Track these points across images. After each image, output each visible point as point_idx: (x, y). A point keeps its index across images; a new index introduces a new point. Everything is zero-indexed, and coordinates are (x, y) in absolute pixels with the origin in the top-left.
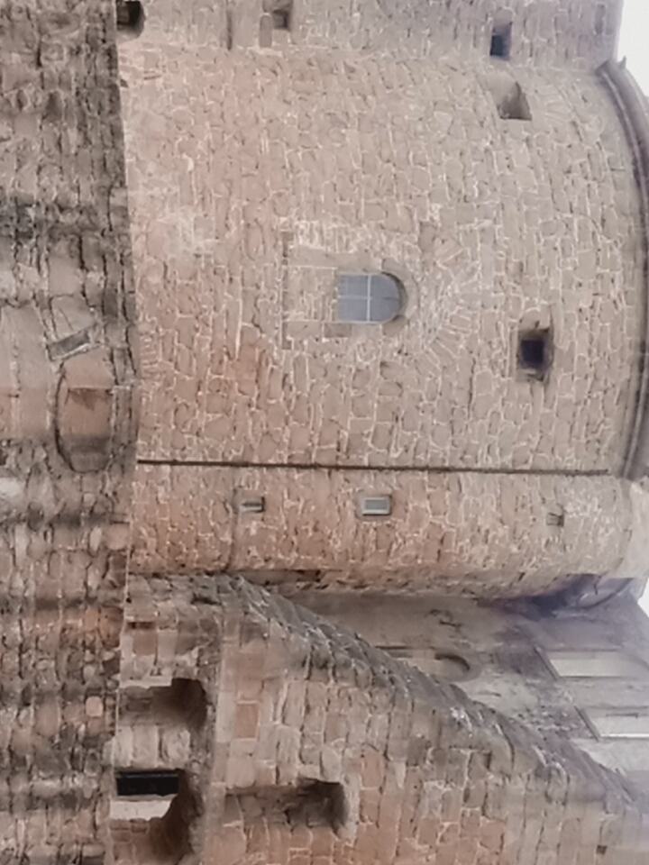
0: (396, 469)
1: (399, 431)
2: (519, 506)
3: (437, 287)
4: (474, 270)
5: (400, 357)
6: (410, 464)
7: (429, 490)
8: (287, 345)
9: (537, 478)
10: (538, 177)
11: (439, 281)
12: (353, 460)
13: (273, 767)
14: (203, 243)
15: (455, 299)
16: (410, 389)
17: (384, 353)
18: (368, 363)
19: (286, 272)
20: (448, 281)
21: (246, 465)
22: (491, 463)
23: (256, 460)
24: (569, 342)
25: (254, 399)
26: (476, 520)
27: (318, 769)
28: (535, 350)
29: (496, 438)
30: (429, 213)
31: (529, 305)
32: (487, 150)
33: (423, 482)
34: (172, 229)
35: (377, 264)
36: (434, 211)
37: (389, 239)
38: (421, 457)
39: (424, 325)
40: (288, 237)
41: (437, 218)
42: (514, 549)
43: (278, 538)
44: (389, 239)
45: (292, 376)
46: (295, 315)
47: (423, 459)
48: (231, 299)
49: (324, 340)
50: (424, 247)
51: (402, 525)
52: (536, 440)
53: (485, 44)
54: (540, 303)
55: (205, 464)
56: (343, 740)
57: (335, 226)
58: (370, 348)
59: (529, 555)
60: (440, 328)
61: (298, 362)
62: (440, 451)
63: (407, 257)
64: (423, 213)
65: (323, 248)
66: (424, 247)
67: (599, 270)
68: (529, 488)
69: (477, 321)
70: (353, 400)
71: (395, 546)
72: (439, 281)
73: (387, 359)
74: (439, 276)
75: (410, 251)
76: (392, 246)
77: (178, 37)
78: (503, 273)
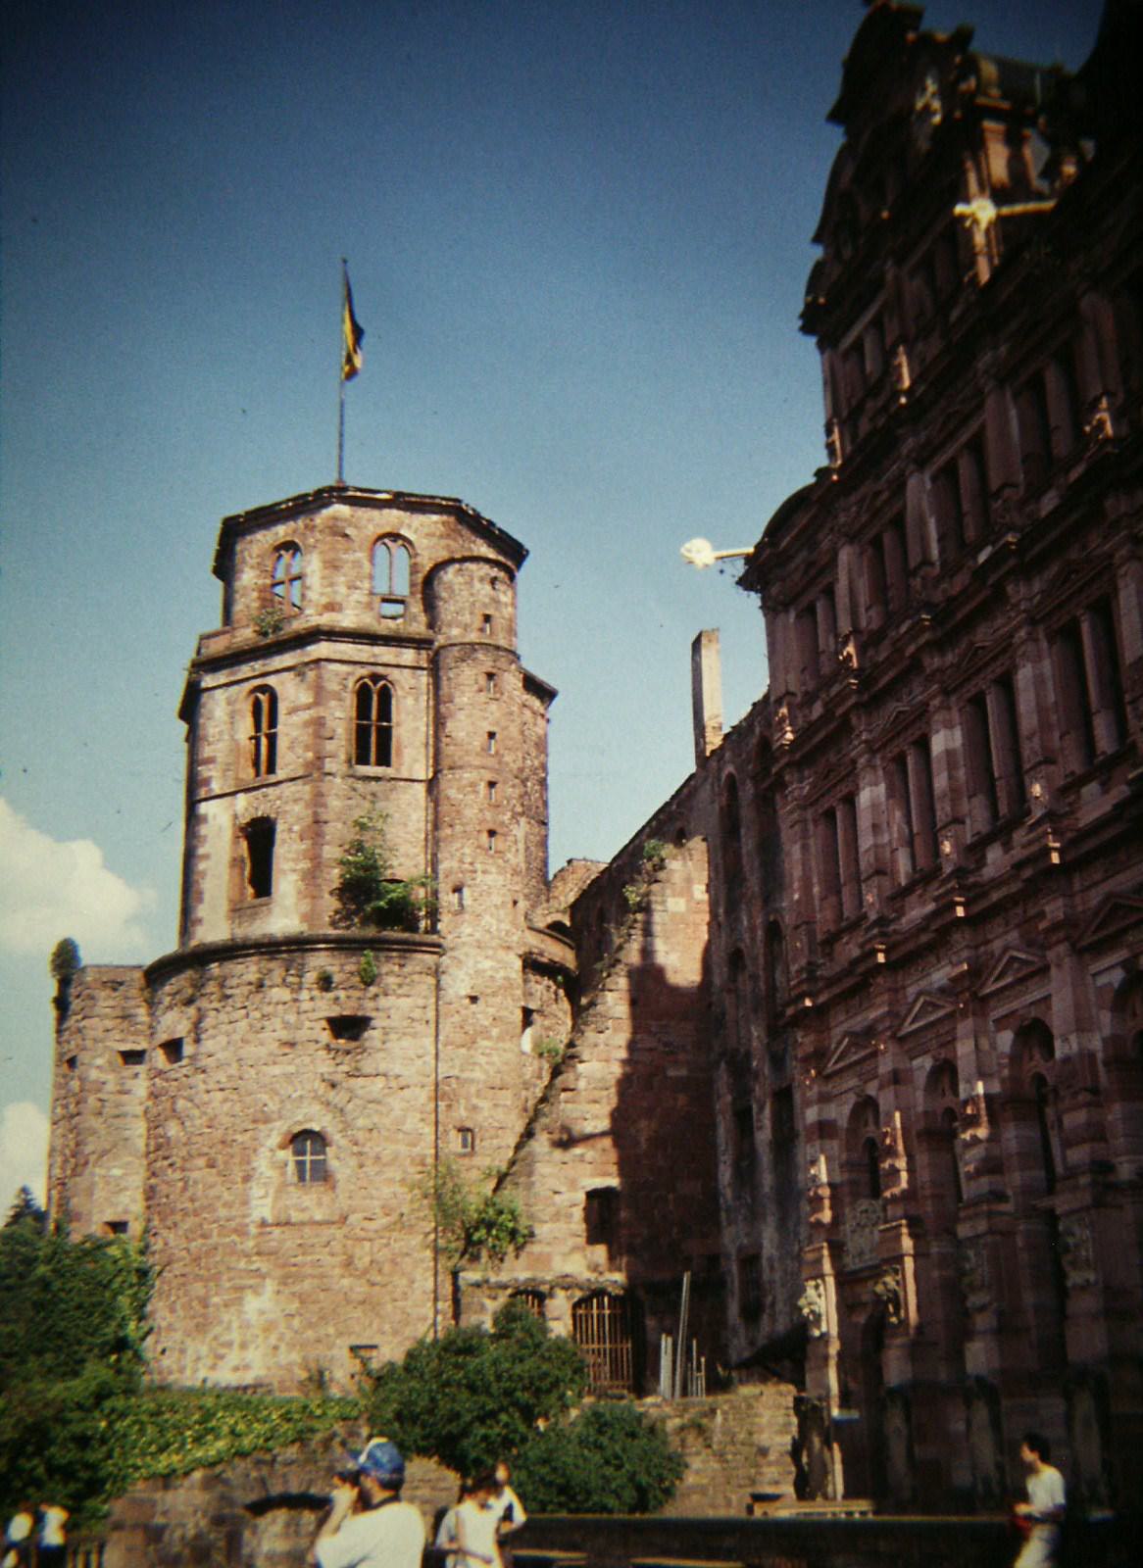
6: (433, 1116)
12: (430, 1161)
14: (270, 1286)
27: (574, 1209)
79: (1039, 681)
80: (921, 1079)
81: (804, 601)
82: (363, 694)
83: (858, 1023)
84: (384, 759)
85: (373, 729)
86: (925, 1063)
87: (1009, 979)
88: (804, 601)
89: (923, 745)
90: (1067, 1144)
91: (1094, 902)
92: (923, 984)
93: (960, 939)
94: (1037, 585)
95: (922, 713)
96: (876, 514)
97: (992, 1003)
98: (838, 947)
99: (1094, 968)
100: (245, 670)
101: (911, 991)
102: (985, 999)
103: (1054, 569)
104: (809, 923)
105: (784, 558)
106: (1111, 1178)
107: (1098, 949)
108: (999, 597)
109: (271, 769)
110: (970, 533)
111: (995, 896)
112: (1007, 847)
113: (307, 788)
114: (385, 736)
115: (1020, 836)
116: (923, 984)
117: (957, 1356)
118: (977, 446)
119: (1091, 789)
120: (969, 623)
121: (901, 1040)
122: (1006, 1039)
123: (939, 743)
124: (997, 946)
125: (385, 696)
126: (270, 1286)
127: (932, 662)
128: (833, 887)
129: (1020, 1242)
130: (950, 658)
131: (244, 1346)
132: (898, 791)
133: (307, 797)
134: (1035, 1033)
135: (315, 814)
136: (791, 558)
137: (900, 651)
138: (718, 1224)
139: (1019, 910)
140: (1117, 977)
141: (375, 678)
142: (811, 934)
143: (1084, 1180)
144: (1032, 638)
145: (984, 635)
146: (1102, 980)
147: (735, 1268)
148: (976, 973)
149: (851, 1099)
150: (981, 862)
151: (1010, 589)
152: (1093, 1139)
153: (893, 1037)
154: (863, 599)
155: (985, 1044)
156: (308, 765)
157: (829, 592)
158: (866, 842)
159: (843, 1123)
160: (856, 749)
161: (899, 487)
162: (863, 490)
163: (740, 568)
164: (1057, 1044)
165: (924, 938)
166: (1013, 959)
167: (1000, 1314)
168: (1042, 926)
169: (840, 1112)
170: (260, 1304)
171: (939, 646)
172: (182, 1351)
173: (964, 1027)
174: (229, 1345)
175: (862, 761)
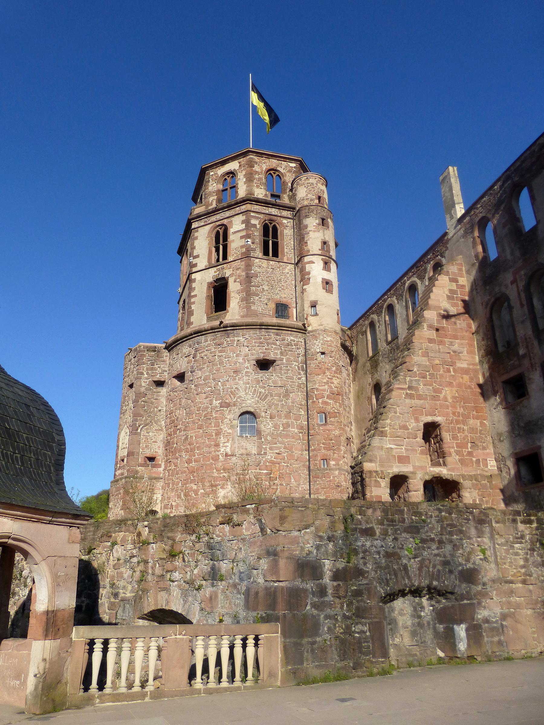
0: (308, 412)
3: (243, 400)
4: (236, 388)
5: (268, 412)
6: (306, 407)
7: (315, 400)
8: (265, 453)
9: (308, 362)
10: (204, 368)
11: (241, 400)
12: (306, 427)
13: (420, 448)
15: (246, 394)
16: (279, 408)
17: (267, 418)
18: (270, 423)
19: (240, 454)
20: (240, 397)
21: (309, 467)
22: (304, 379)
23: (308, 463)
25: (285, 465)
26: (324, 383)
28: (264, 365)
29: (295, 377)
30: (217, 405)
31: (247, 368)
32: (195, 386)
33: (312, 402)
36: (216, 403)
37: (227, 418)
38: (303, 403)
39: (256, 404)
41: (219, 402)
42: (334, 369)
43: (335, 453)
44: (227, 418)
45: (276, 451)
47: (304, 402)
49: (263, 440)
50: (228, 405)
52: (295, 363)
53: (159, 389)
54: (247, 364)
55: (310, 482)
56: (407, 423)
57: (222, 438)
58: (265, 423)
59: (335, 363)
60: (257, 399)
62: (299, 397)
63: (232, 412)
64: (217, 406)
65: (230, 441)
66: (228, 405)
67: (235, 345)
69: (254, 386)
70: (284, 428)
71: (336, 411)
72: (241, 400)
73: (269, 417)
74: (239, 400)
75: (230, 411)
76: (228, 417)
78: (237, 378)
82: (266, 228)
84: (276, 254)
85: (271, 242)
100: (213, 219)
109: (225, 257)
113: (243, 263)
125: (275, 229)
133: (243, 267)
135: (247, 274)
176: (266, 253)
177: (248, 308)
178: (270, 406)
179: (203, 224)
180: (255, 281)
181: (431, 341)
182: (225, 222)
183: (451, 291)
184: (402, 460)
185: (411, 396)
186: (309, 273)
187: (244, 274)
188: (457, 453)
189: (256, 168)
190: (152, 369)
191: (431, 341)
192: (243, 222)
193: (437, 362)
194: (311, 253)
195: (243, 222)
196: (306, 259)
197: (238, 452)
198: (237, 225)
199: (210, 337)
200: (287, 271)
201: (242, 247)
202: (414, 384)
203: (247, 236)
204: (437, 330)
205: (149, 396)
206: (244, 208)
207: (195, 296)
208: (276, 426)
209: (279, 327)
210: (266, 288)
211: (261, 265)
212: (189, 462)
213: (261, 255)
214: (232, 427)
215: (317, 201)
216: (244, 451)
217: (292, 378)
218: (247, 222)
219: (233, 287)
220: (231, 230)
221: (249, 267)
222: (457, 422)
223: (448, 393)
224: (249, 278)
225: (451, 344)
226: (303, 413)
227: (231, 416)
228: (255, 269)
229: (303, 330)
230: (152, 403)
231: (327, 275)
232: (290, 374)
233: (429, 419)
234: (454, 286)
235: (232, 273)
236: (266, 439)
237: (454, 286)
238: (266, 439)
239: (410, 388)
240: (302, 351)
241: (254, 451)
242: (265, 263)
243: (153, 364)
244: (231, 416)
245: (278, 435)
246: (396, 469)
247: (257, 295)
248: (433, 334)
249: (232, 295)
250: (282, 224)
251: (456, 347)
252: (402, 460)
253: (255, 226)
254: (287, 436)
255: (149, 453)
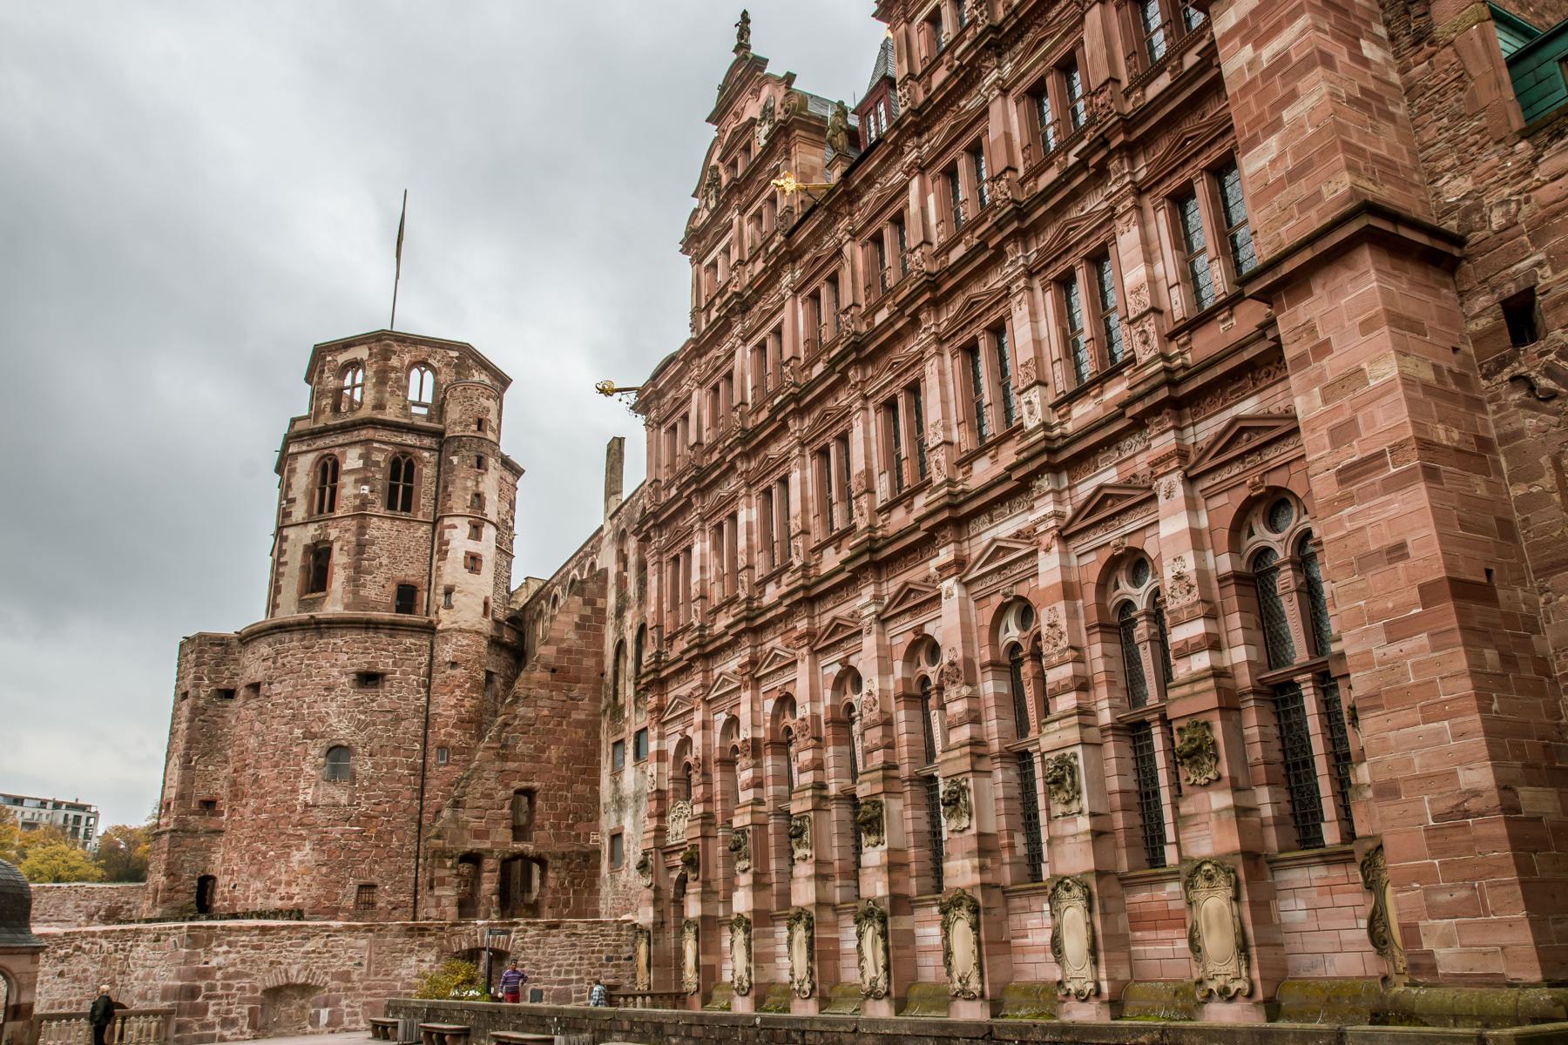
1: (406, 746)
2: (445, 684)
14: (308, 846)
16: (384, 742)
24: (362, 662)
28: (369, 679)
34: (301, 862)
35: (321, 760)
40: (307, 805)
46: (344, 800)
48: (336, 832)
50: (314, 736)
51: (453, 742)
59: (471, 678)
61: (367, 798)
62: (414, 725)
66: (314, 736)
68: (438, 678)
77: (217, 858)
79: (803, 482)
80: (719, 726)
81: (670, 423)
82: (395, 464)
83: (684, 690)
84: (407, 507)
86: (721, 718)
87: (773, 668)
88: (670, 423)
89: (733, 517)
90: (801, 771)
91: (826, 622)
92: (723, 669)
93: (746, 641)
94: (807, 422)
95: (733, 498)
96: (717, 370)
97: (764, 682)
98: (676, 643)
99: (823, 663)
100: (320, 443)
101: (717, 672)
102: (759, 679)
103: (816, 414)
104: (659, 627)
105: (660, 394)
106: (825, 793)
107: (826, 650)
108: (784, 427)
109: (332, 509)
110: (770, 388)
111: (769, 615)
112: (778, 583)
114: (408, 492)
115: (785, 579)
116: (723, 669)
117: (728, 900)
118: (778, 332)
119: (830, 551)
120: (764, 444)
121: (709, 702)
122: (769, 705)
123: (742, 518)
124: (768, 647)
125: (410, 466)
126: (308, 846)
127: (741, 466)
128: (675, 605)
129: (771, 830)
130: (753, 464)
131: (289, 884)
132: (717, 547)
134: (786, 702)
136: (664, 395)
137: (723, 458)
138: (598, 813)
139: (782, 625)
140: (837, 668)
141: (405, 454)
142: (660, 634)
143: (809, 793)
144: (802, 455)
145: (775, 450)
146: (827, 671)
147: (607, 841)
148: (753, 662)
149: (678, 737)
150: (763, 593)
151: (790, 422)
152: (815, 769)
153: (704, 700)
154: (706, 423)
155: (757, 707)
156: (355, 508)
157: (686, 418)
158: (696, 577)
159: (672, 752)
160: (692, 517)
161: (731, 355)
162: (710, 355)
163: (632, 397)
164: (798, 708)
165: (726, 639)
166: (777, 655)
167: (755, 874)
168: (795, 635)
169: (671, 745)
170: (303, 855)
171: (746, 456)
172: (248, 886)
173: (746, 696)
174: (279, 883)
175: (697, 526)
176: (391, 505)
177: (356, 593)
178: (371, 739)
179: (305, 448)
180: (370, 551)
181: (541, 685)
182: (337, 451)
183: (582, 617)
184: (480, 834)
185: (504, 758)
186: (447, 543)
187: (353, 539)
188: (553, 826)
189: (394, 362)
190: (216, 672)
191: (541, 685)
192: (360, 457)
193: (546, 712)
194: (455, 512)
195: (360, 457)
196: (447, 521)
197: (321, 802)
198: (352, 460)
199: (296, 636)
200: (420, 533)
201: (356, 496)
202: (510, 742)
203: (365, 481)
204: (554, 671)
205: (210, 713)
206: (365, 434)
207: (285, 563)
208: (375, 766)
209: (394, 627)
210: (385, 561)
211: (381, 528)
212: (258, 811)
213: (382, 512)
214: (316, 767)
215: (474, 427)
216: (329, 801)
217: (406, 699)
218: (365, 457)
219: (339, 559)
220: (345, 467)
221: (362, 529)
222: (560, 788)
223: (554, 752)
224: (361, 547)
225: (570, 690)
226: (418, 747)
227: (316, 752)
228: (372, 532)
229: (430, 629)
230: (215, 723)
231: (473, 547)
232: (404, 693)
233: (524, 784)
234: (588, 611)
235: (340, 535)
236: (361, 785)
237: (588, 611)
238: (361, 785)
239: (504, 746)
240: (425, 659)
241: (344, 800)
242: (387, 524)
243: (218, 665)
244: (316, 751)
245: (379, 779)
246: (472, 845)
247: (371, 573)
248: (547, 676)
249: (336, 569)
250: (420, 459)
251: (575, 693)
252: (480, 834)
253: (377, 464)
254: (391, 780)
255: (204, 794)
